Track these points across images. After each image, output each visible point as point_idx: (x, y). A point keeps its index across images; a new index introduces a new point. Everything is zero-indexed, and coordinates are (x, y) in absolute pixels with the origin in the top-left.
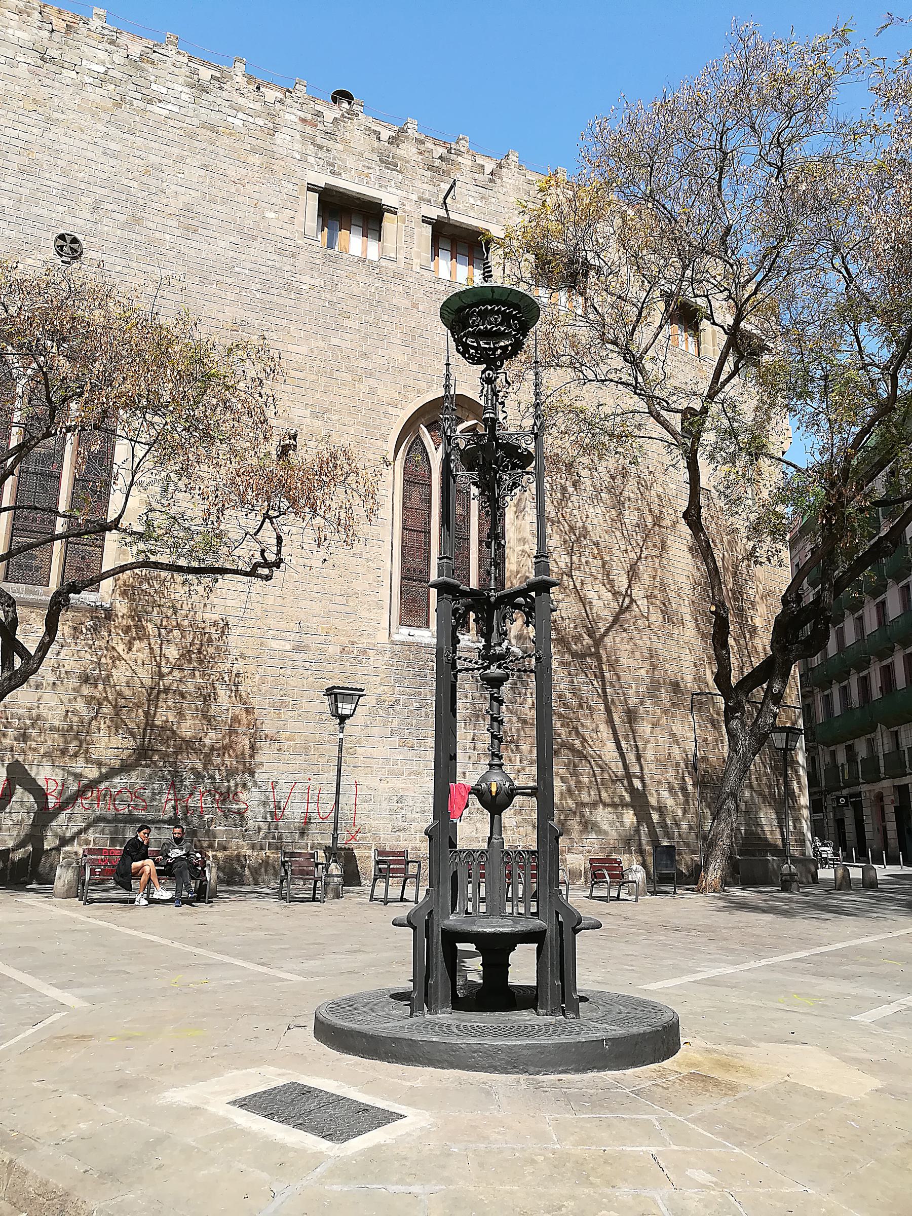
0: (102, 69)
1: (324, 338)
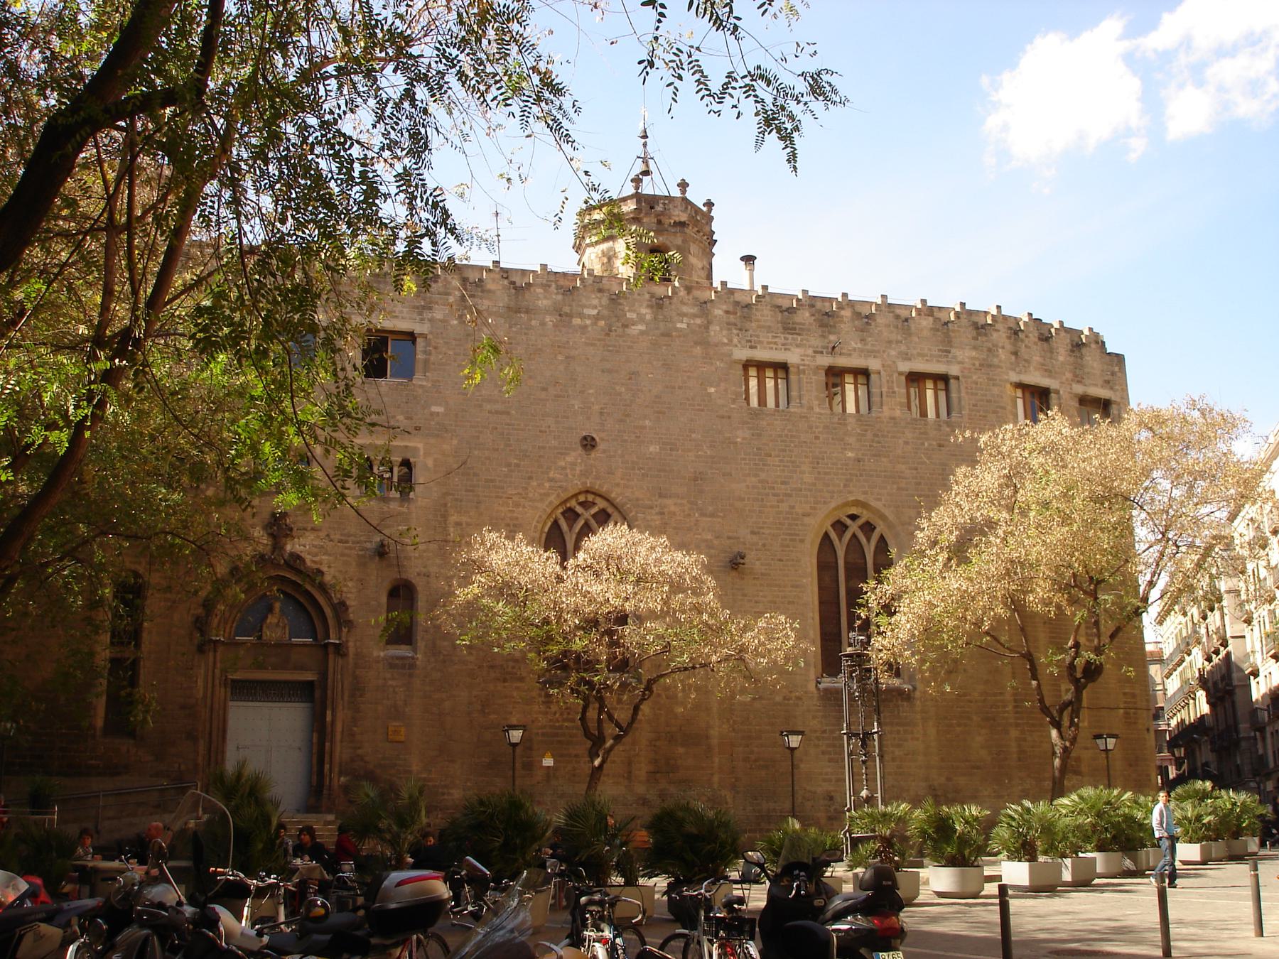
0: (594, 312)
1: (756, 475)
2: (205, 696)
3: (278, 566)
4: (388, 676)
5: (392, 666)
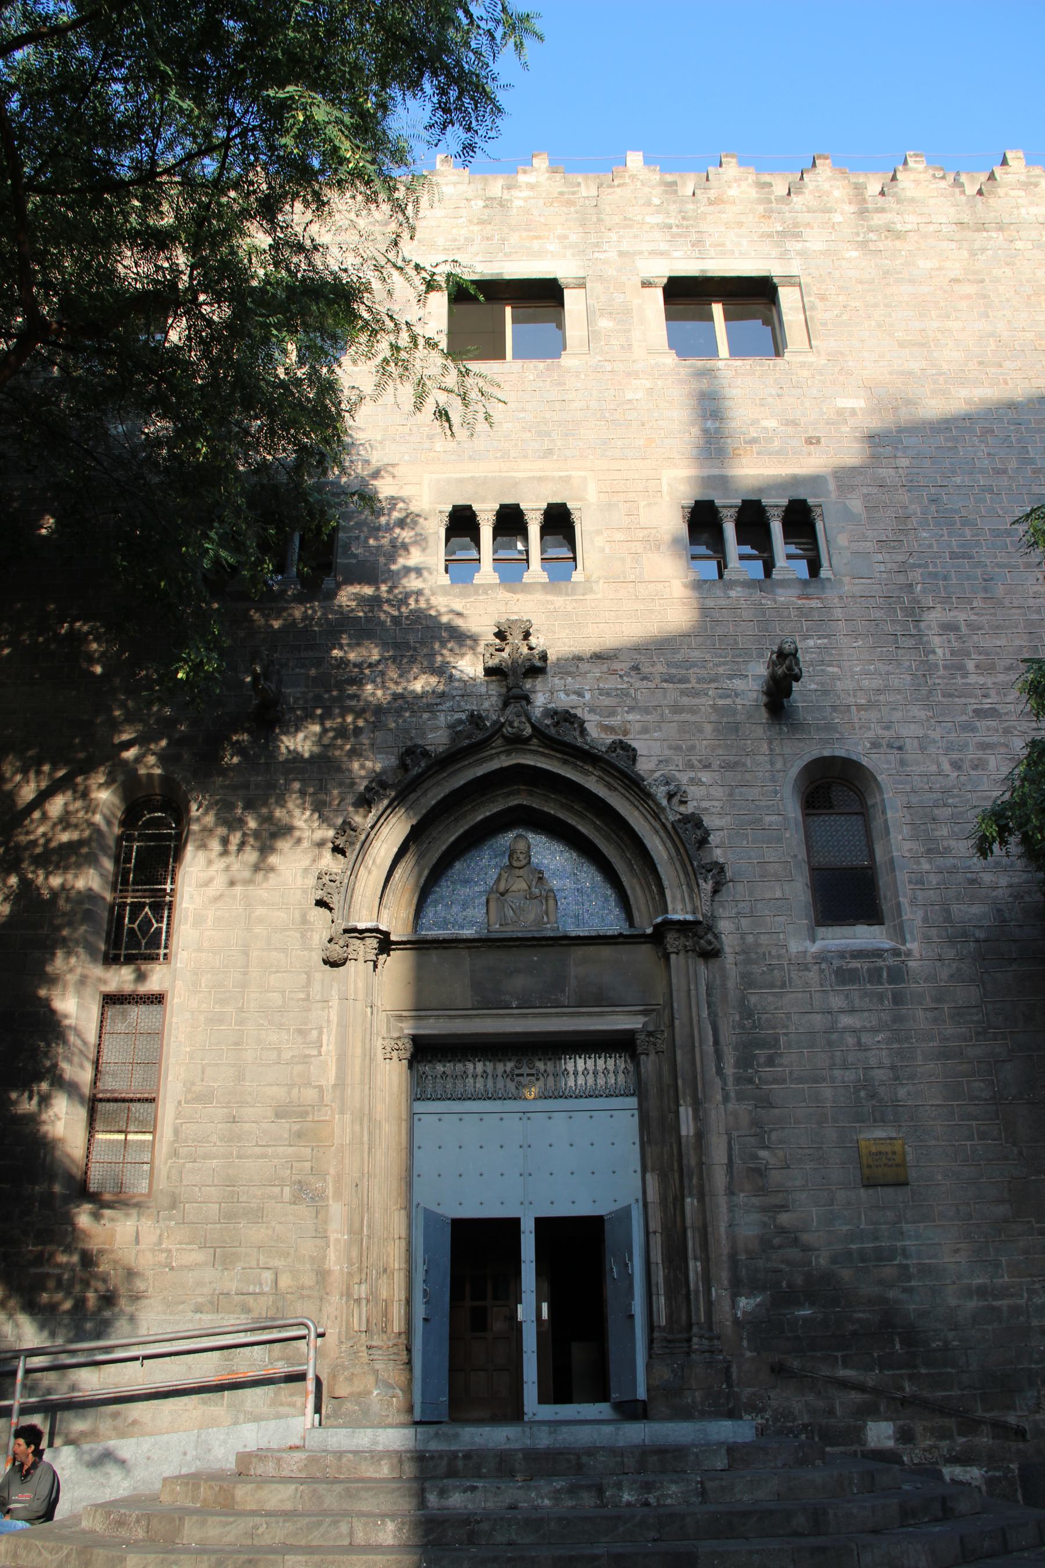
2: (340, 1084)
3: (516, 742)
4: (836, 1002)
5: (845, 977)
